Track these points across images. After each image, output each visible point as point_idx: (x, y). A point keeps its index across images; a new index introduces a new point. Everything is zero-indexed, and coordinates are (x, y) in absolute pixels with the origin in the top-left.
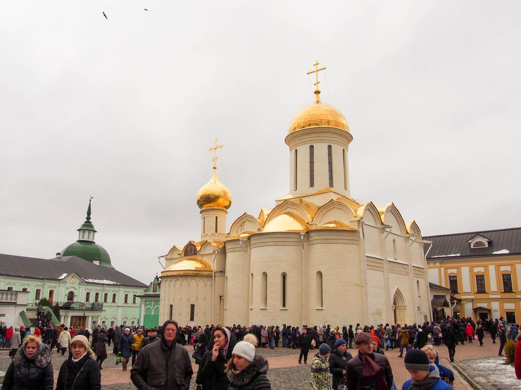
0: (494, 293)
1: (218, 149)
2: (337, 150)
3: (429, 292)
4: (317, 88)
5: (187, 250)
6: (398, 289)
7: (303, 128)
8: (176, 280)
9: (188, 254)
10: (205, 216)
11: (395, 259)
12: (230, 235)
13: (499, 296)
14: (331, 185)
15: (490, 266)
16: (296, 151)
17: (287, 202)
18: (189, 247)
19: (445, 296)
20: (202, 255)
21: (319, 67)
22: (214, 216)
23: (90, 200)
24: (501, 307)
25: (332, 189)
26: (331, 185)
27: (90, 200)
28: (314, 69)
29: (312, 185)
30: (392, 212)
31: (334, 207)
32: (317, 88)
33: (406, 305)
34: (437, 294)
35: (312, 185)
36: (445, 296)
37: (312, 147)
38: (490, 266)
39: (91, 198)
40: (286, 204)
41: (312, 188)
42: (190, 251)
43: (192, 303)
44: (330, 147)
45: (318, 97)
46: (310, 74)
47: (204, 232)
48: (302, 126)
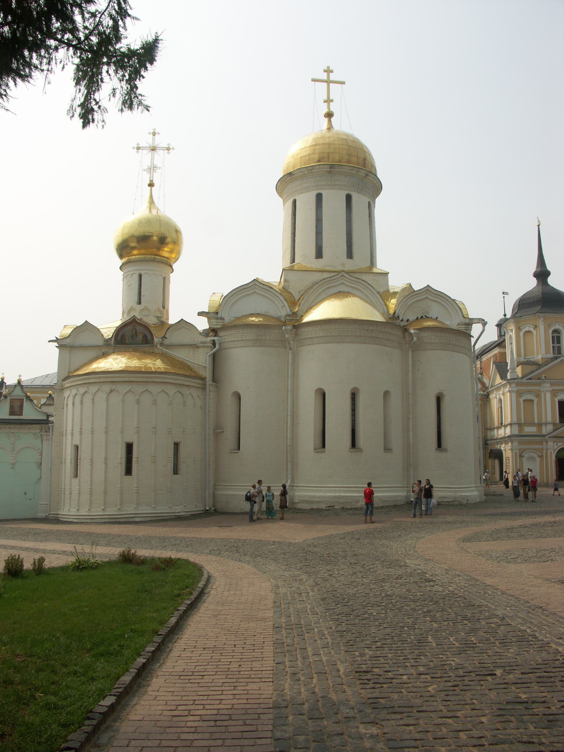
1: (161, 152)
4: (329, 107)
5: (121, 333)
7: (337, 162)
8: (142, 392)
9: (127, 342)
10: (142, 273)
12: (219, 315)
16: (319, 197)
17: (343, 275)
18: (130, 328)
20: (169, 346)
21: (333, 77)
22: (155, 274)
28: (324, 76)
31: (427, 298)
40: (341, 278)
42: (132, 337)
43: (177, 440)
45: (330, 121)
47: (139, 303)
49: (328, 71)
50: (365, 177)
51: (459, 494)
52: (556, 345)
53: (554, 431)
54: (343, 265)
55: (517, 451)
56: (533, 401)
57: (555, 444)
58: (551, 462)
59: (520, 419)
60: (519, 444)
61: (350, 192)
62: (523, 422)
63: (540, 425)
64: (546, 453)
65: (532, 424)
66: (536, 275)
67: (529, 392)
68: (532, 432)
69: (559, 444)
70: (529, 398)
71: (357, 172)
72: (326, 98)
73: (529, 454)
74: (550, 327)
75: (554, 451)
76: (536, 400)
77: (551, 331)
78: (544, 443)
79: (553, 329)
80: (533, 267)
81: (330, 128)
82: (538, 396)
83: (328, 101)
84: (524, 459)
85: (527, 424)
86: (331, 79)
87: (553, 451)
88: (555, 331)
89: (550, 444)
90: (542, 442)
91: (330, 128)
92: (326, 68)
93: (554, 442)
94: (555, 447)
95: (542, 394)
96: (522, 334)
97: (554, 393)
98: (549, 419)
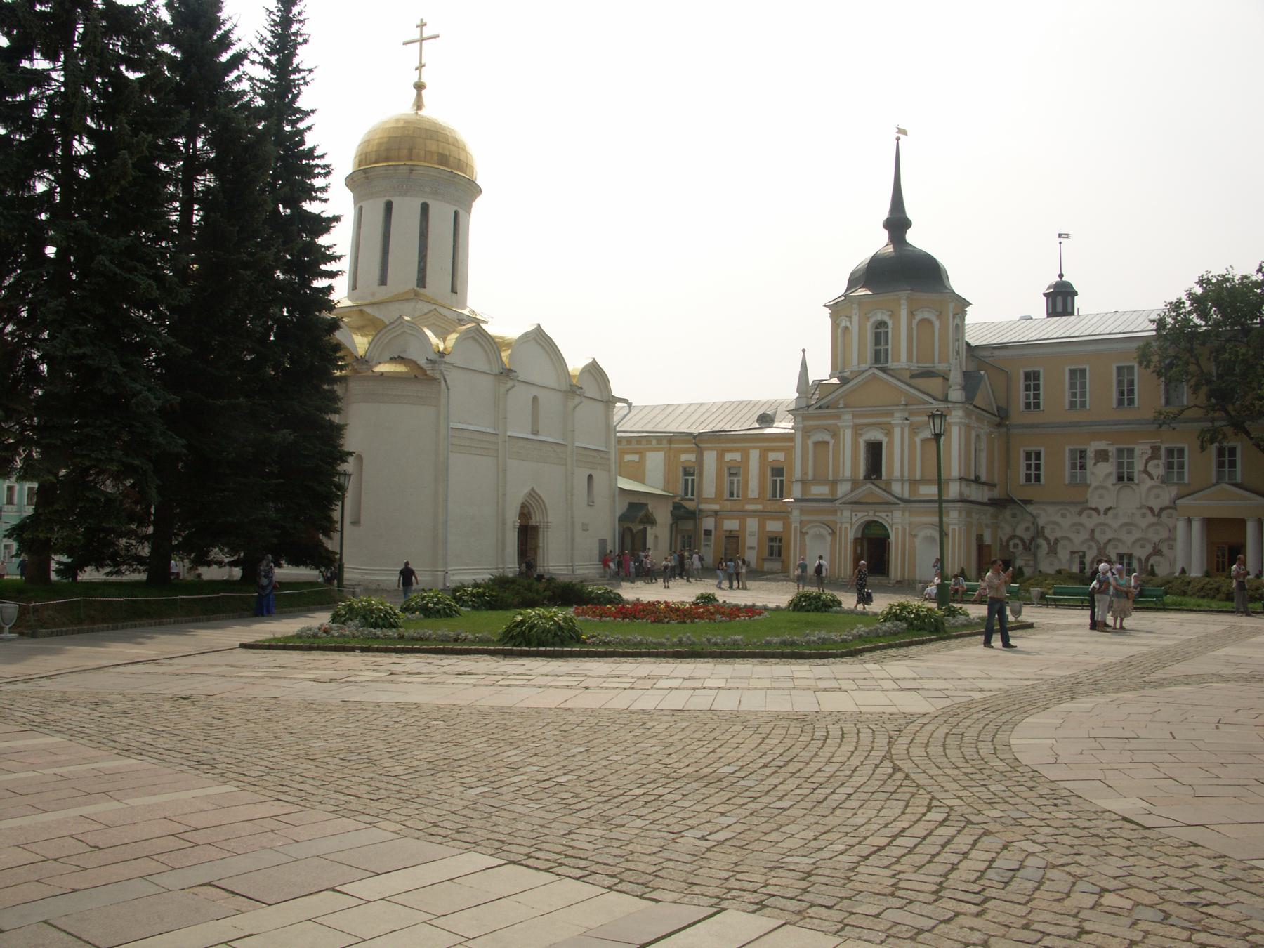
0: (753, 501)
2: (440, 214)
3: (617, 498)
4: (420, 78)
6: (532, 489)
11: (533, 433)
13: (759, 507)
14: (422, 281)
15: (751, 451)
19: (647, 505)
21: (427, 32)
24: (762, 526)
25: (421, 291)
26: (422, 281)
29: (383, 281)
30: (536, 341)
32: (420, 78)
33: (549, 520)
34: (637, 502)
35: (383, 281)
36: (647, 505)
37: (389, 206)
38: (751, 451)
41: (383, 287)
44: (425, 208)
46: (408, 45)
48: (374, 159)
49: (422, 25)
51: (366, 577)
52: (882, 347)
53: (852, 491)
54: (373, 295)
55: (798, 525)
56: (828, 443)
57: (854, 514)
58: (846, 544)
59: (806, 474)
60: (801, 514)
61: (390, 199)
62: (810, 476)
63: (834, 483)
64: (840, 528)
65: (824, 482)
66: (888, 225)
67: (818, 428)
68: (821, 494)
69: (860, 515)
70: (821, 440)
72: (417, 64)
73: (816, 529)
74: (868, 318)
75: (851, 524)
76: (832, 442)
77: (869, 325)
78: (839, 514)
79: (872, 320)
80: (884, 212)
81: (419, 105)
82: (835, 435)
83: (420, 67)
84: (807, 538)
85: (817, 481)
86: (425, 35)
87: (849, 527)
88: (882, 324)
89: (847, 513)
90: (836, 511)
91: (419, 105)
92: (424, 21)
93: (852, 511)
94: (854, 519)
95: (842, 430)
96: (839, 331)
97: (857, 430)
98: (848, 474)
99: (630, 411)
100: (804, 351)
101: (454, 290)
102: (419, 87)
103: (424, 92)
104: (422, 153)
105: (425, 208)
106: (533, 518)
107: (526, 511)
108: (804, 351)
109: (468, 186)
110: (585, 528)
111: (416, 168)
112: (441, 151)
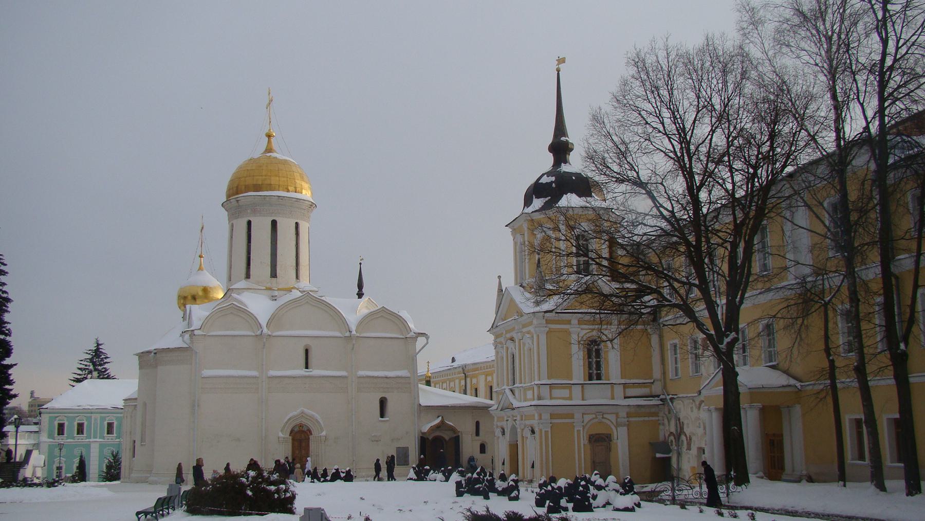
23: (360, 264)
27: (360, 264)
39: (361, 260)
44: (249, 223)
50: (238, 203)
71: (231, 203)
81: (269, 150)
99: (427, 343)
100: (499, 277)
101: (274, 275)
102: (269, 136)
103: (272, 140)
104: (243, 187)
105: (249, 223)
106: (313, 433)
107: (305, 429)
108: (499, 277)
109: (281, 200)
110: (376, 440)
111: (239, 199)
112: (255, 183)
